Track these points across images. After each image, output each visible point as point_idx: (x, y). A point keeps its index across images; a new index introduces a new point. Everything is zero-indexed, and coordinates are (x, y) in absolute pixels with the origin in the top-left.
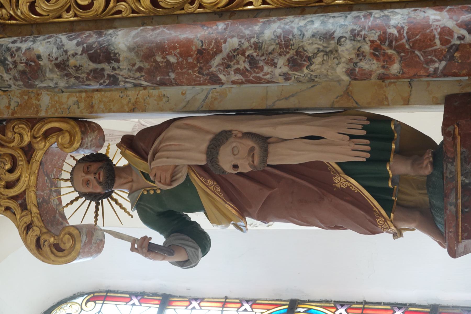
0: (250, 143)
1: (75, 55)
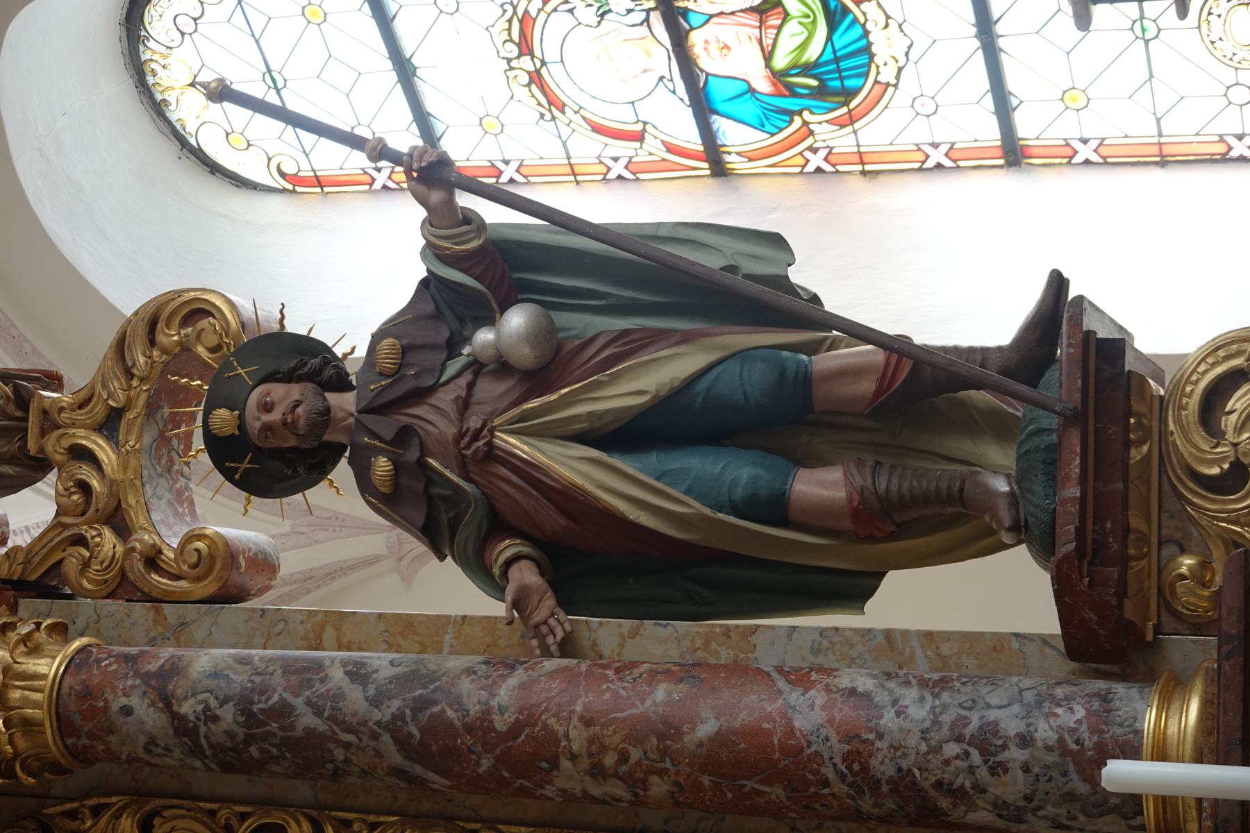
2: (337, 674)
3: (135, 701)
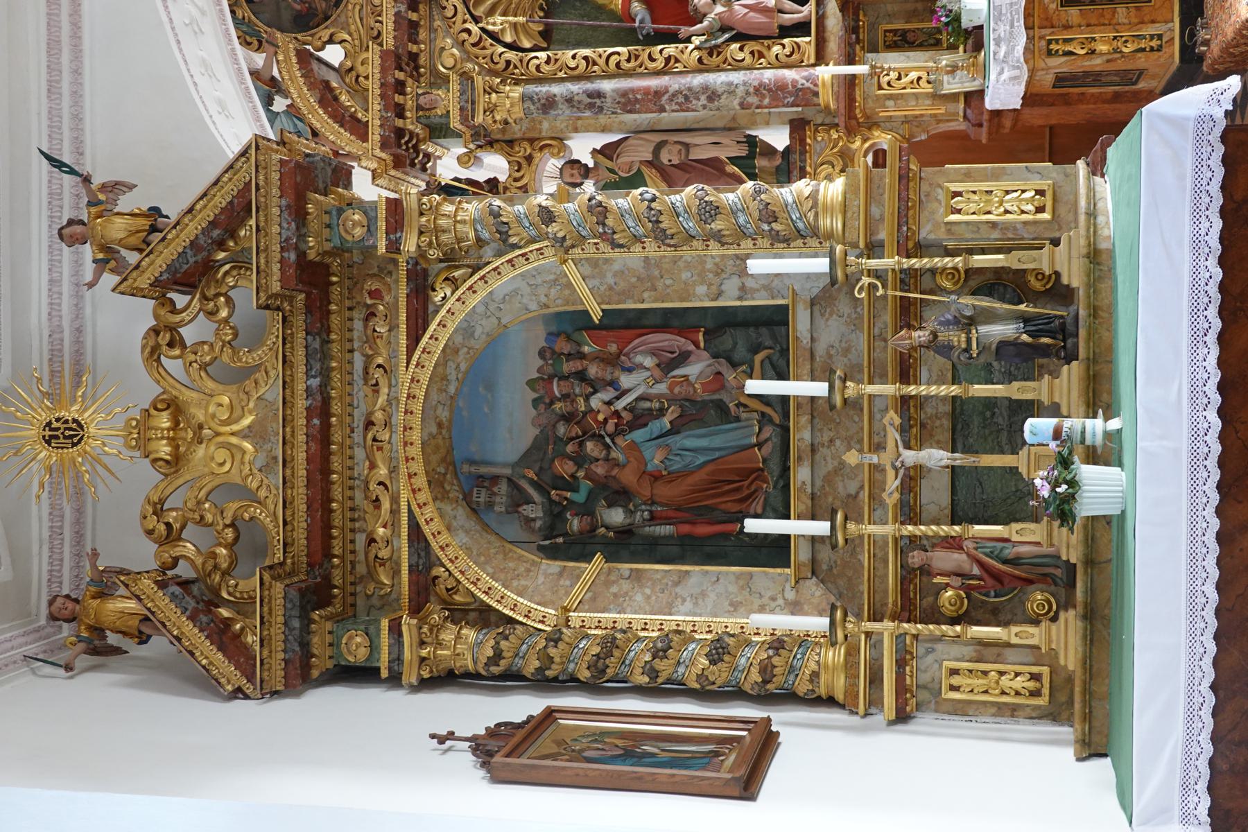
0: (679, 147)
1: (578, 94)
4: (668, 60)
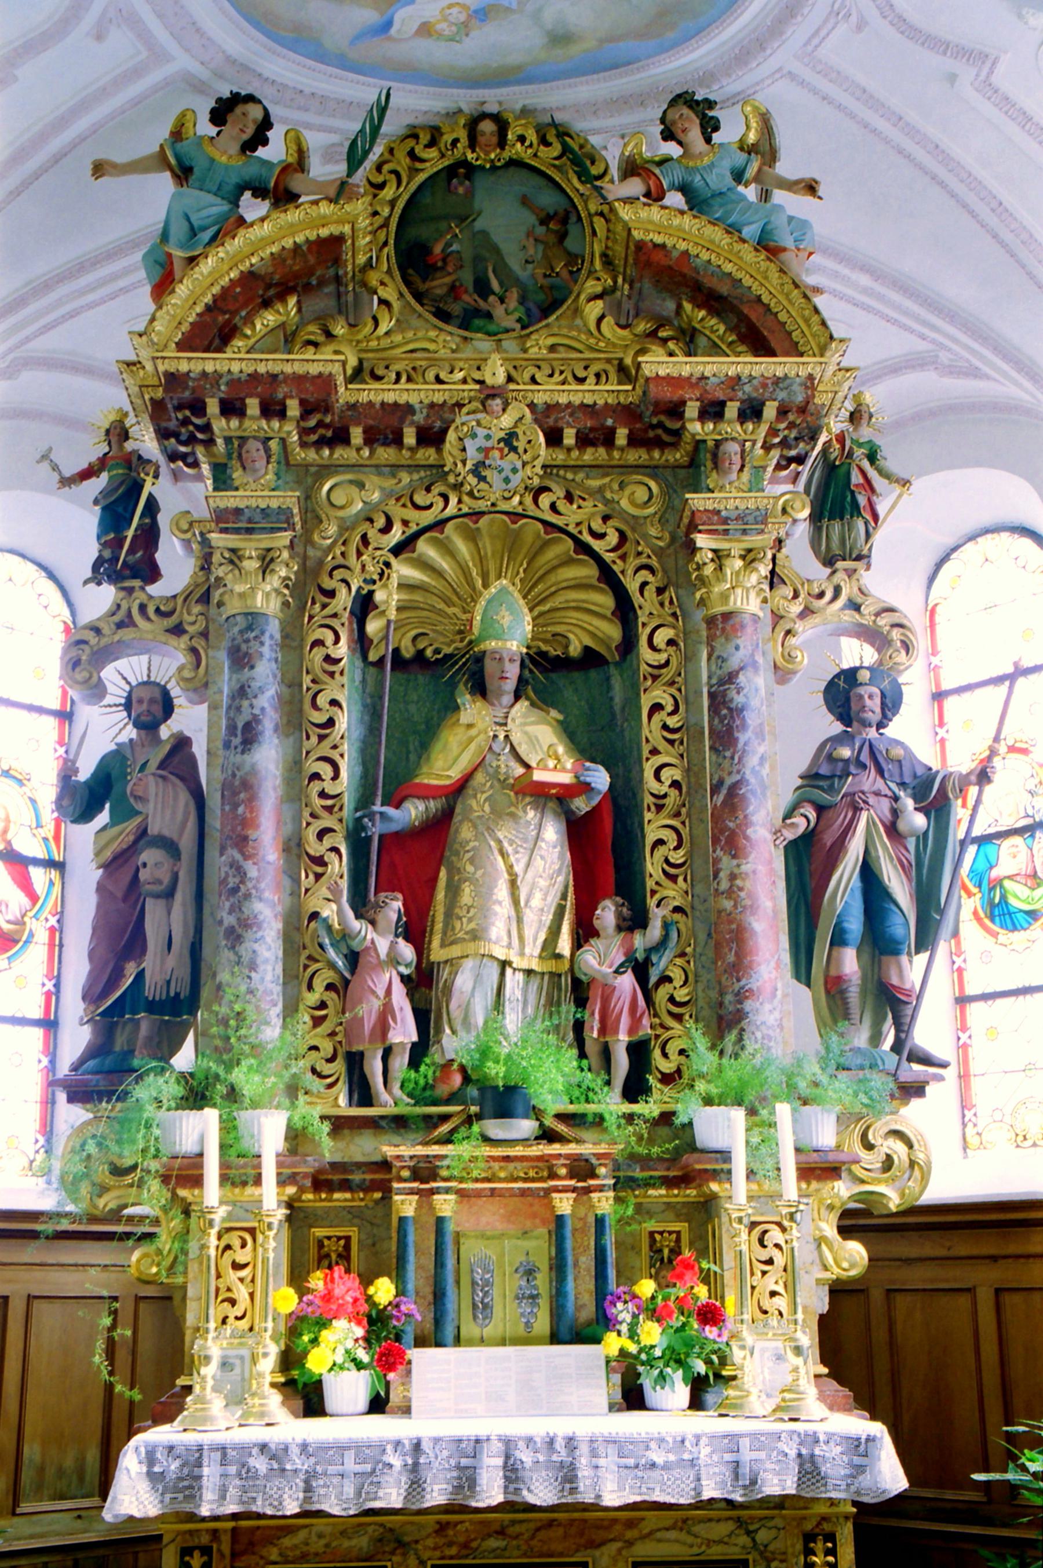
0: (166, 880)
1: (252, 706)
2: (761, 749)
3: (742, 652)
4: (320, 861)
